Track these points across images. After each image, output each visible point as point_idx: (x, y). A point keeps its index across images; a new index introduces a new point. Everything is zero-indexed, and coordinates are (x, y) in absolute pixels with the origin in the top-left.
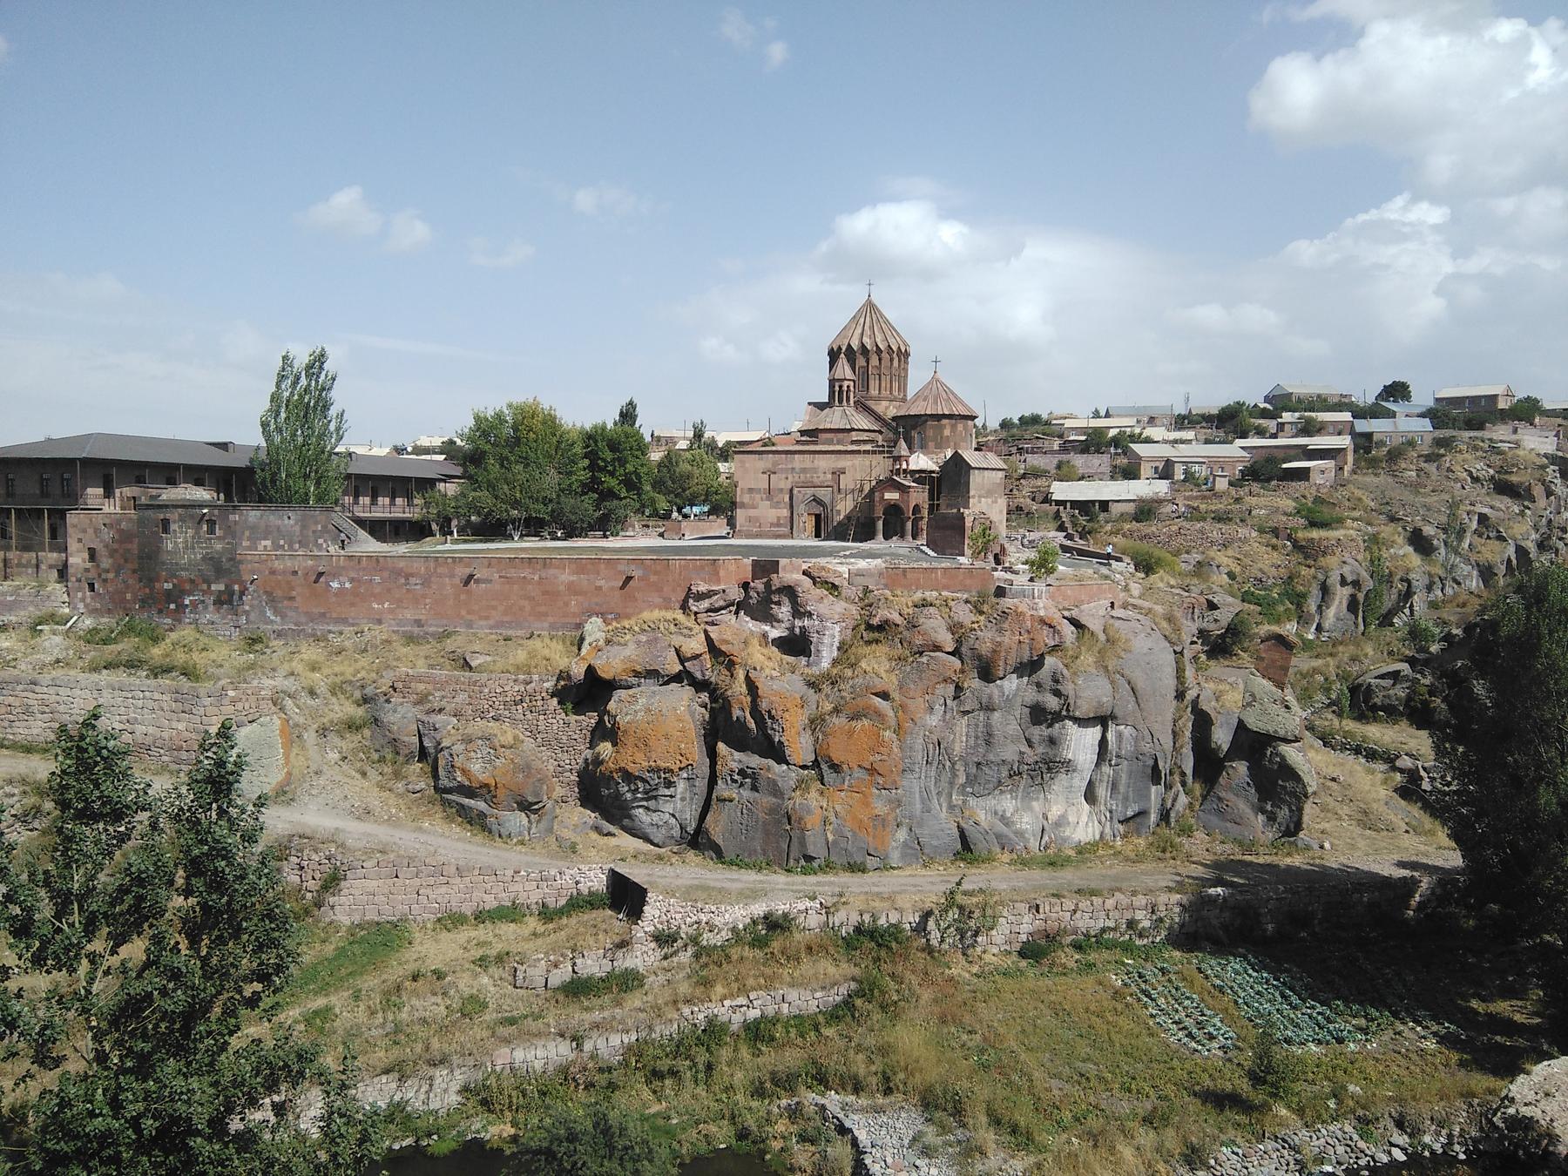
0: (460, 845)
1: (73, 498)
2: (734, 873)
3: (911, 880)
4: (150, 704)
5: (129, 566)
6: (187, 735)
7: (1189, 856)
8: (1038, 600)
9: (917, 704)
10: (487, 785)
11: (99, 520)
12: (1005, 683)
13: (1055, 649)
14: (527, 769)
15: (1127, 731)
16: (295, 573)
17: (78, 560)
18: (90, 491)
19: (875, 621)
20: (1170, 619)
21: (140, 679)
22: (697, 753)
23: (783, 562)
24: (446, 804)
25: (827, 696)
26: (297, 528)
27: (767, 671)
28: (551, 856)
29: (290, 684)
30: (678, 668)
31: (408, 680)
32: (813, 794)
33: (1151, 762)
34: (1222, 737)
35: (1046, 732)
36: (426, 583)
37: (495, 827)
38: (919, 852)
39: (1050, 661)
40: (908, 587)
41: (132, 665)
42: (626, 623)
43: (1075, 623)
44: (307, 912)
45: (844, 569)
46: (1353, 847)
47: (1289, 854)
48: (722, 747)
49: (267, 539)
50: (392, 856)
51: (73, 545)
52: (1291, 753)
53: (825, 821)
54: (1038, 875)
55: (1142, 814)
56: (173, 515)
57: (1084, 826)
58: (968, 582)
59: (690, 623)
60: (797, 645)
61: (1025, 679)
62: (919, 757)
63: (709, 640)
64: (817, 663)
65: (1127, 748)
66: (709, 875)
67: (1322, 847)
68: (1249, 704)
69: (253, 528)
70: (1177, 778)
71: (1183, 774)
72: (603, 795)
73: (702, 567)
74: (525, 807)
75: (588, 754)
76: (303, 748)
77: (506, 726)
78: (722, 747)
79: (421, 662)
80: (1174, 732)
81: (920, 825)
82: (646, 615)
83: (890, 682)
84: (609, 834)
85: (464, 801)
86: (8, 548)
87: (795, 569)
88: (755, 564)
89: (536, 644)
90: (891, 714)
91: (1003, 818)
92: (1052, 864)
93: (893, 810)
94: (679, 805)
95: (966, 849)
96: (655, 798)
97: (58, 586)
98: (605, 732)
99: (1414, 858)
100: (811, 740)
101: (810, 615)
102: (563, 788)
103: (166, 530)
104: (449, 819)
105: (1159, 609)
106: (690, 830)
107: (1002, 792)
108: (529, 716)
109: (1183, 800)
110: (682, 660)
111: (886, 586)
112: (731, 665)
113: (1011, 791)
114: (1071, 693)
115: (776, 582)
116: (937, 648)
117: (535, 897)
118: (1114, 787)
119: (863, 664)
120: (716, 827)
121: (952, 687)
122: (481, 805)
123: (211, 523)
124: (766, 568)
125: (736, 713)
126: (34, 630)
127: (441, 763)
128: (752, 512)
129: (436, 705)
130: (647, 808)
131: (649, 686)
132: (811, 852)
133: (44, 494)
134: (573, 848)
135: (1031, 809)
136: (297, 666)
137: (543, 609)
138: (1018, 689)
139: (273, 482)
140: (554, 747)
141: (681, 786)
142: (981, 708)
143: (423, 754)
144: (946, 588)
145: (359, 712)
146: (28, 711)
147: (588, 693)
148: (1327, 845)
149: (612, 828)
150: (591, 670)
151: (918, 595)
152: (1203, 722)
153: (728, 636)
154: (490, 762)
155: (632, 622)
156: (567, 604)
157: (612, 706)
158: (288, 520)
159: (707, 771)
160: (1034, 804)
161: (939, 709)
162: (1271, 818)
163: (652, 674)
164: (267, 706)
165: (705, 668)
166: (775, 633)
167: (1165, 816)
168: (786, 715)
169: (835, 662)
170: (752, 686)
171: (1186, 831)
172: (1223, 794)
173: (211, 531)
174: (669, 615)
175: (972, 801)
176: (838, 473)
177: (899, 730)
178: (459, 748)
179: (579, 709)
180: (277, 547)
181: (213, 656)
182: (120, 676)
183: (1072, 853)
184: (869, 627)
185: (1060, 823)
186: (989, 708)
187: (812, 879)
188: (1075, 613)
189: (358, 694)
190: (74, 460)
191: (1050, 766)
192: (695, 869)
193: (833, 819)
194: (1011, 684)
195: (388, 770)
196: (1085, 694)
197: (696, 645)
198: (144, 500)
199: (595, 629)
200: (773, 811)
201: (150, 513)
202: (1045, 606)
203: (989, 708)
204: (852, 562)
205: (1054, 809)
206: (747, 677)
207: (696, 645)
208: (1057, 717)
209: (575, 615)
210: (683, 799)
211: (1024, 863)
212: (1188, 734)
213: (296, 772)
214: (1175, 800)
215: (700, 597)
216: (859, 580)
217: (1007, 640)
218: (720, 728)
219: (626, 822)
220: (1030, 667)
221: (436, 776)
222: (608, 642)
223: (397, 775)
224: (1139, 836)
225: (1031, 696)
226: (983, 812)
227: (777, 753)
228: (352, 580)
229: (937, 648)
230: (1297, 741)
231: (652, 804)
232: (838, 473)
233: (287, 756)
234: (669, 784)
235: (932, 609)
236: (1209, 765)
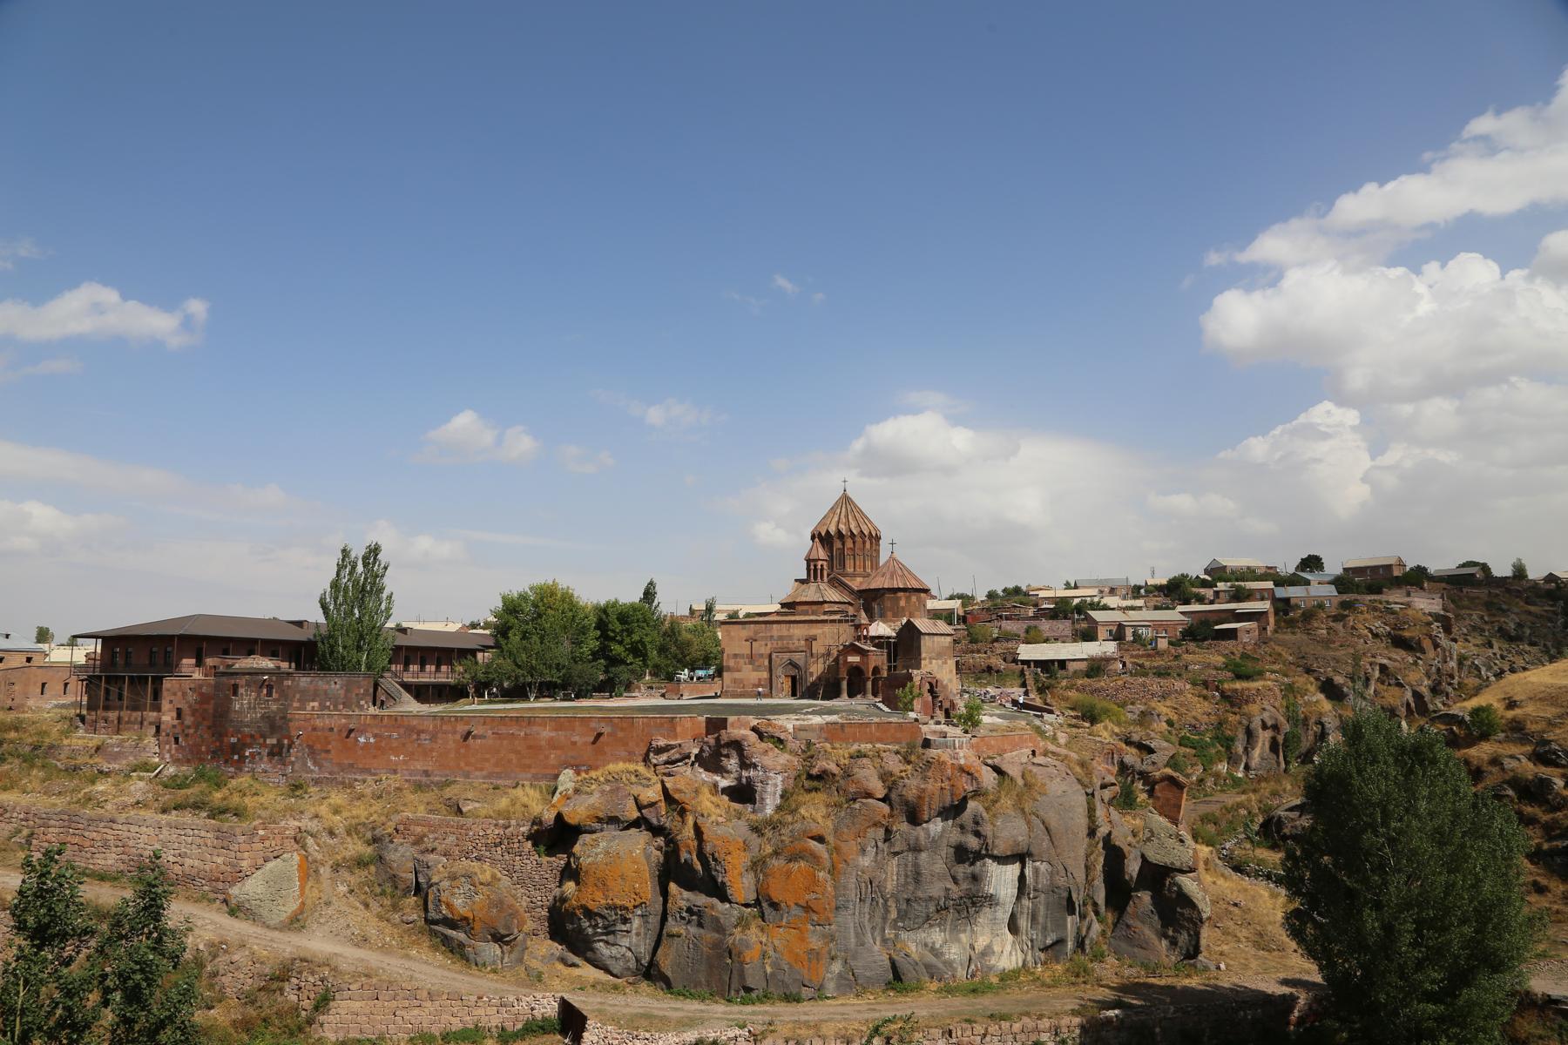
0: (439, 972)
1: (170, 667)
2: (679, 1004)
3: (841, 1009)
4: (198, 841)
5: (206, 723)
6: (223, 868)
7: (1099, 980)
8: (958, 747)
9: (850, 847)
10: (466, 919)
11: (187, 684)
12: (931, 826)
13: (978, 793)
14: (499, 904)
15: (1043, 867)
16: (331, 729)
17: (168, 718)
18: (185, 661)
19: (814, 771)
20: (1082, 764)
21: (201, 819)
22: (649, 890)
23: (731, 719)
24: (435, 934)
25: (769, 840)
26: (342, 692)
27: (713, 818)
28: (519, 983)
29: (313, 826)
30: (636, 814)
31: (407, 823)
32: (754, 930)
33: (1065, 895)
34: (1133, 868)
35: (970, 870)
36: (433, 738)
37: (472, 956)
38: (852, 983)
39: (971, 804)
40: (845, 740)
41: (197, 806)
42: (593, 774)
43: (998, 770)
44: (300, 1029)
45: (790, 727)
46: (1246, 967)
47: (1188, 976)
48: (673, 887)
49: (317, 703)
50: (374, 980)
51: (165, 706)
52: (1187, 883)
53: (764, 955)
54: (958, 1002)
55: (1060, 942)
56: (242, 681)
57: (1008, 954)
58: (899, 735)
59: (649, 773)
60: (743, 793)
61: (950, 822)
62: (853, 895)
63: (665, 790)
64: (762, 809)
65: (1044, 881)
66: (656, 1004)
67: (1218, 968)
68: (1149, 840)
69: (303, 692)
70: (1090, 908)
71: (1095, 904)
72: (571, 930)
73: (662, 725)
74: (498, 938)
75: (557, 892)
76: (318, 881)
77: (486, 866)
78: (673, 887)
79: (422, 808)
80: (1087, 867)
81: (854, 958)
82: (611, 767)
83: (826, 826)
84: (574, 965)
85: (447, 932)
86: (121, 708)
87: (743, 725)
88: (709, 721)
89: (519, 792)
90: (826, 855)
91: (933, 950)
92: (974, 991)
93: (827, 944)
94: (632, 942)
95: (897, 978)
96: (613, 933)
97: (153, 740)
98: (571, 873)
99: (1297, 976)
100: (753, 881)
101: (755, 766)
102: (533, 922)
103: (235, 693)
104: (434, 948)
105: (1074, 756)
106: (645, 962)
107: (931, 926)
108: (507, 857)
109: (1097, 927)
110: (640, 807)
111: (827, 740)
112: (683, 813)
113: (939, 925)
114: (989, 834)
115: (725, 736)
116: (869, 795)
117: (495, 1021)
118: (1034, 918)
119: (802, 811)
120: (666, 962)
121: (881, 832)
122: (460, 936)
123: (270, 688)
124: (715, 725)
125: (684, 856)
126: (128, 776)
127: (431, 897)
128: (737, 675)
129: (430, 846)
130: (607, 942)
131: (611, 831)
132: (750, 983)
133: (152, 664)
134: (539, 978)
135: (959, 940)
136: (323, 809)
137: (527, 761)
138: (944, 830)
139: (332, 653)
140: (528, 885)
141: (636, 922)
142: (909, 850)
143: (418, 889)
144: (880, 740)
145: (369, 851)
146: (106, 846)
147: (557, 837)
148: (1223, 966)
149: (576, 960)
150: (559, 817)
151: (855, 747)
152: (1114, 856)
153: (681, 786)
154: (471, 897)
155: (599, 773)
156: (547, 757)
157: (577, 849)
158: (335, 685)
159: (659, 908)
160: (962, 936)
161: (871, 850)
162: (1174, 943)
163: (613, 820)
164: (290, 844)
165: (662, 816)
166: (724, 783)
167: (1080, 944)
168: (729, 858)
169: (779, 808)
170: (698, 831)
171: (1099, 957)
172: (1131, 922)
173: (269, 694)
174: (632, 767)
175: (904, 935)
176: (810, 640)
177: (833, 871)
178: (445, 884)
179: (551, 852)
180: (323, 707)
181: (262, 799)
182: (187, 817)
183: (995, 980)
184: (810, 777)
185: (987, 952)
186: (916, 849)
187: (749, 1008)
188: (997, 761)
189: (369, 835)
190: (172, 637)
191: (973, 901)
192: (646, 999)
193: (771, 953)
194: (936, 826)
195: (387, 902)
196: (1005, 834)
197: (652, 794)
198: (222, 669)
199: (567, 779)
200: (716, 945)
201: (224, 679)
202: (965, 756)
203: (916, 849)
204: (805, 719)
205: (981, 939)
206: (696, 825)
207: (652, 794)
208: (978, 856)
209: (553, 767)
210: (638, 934)
211: (949, 991)
212: (1099, 867)
213: (309, 902)
214: (1089, 928)
215: (660, 751)
216: (803, 735)
217: (930, 787)
218: (671, 870)
219: (589, 954)
220: (953, 811)
221: (426, 910)
222: (577, 791)
223: (395, 907)
224: (1058, 962)
225: (955, 836)
226: (913, 944)
227: (720, 892)
228: (375, 736)
229: (869, 795)
230: (1192, 870)
231: (610, 938)
232: (810, 640)
233: (302, 888)
234: (625, 921)
235: (865, 761)
236: (1119, 893)
